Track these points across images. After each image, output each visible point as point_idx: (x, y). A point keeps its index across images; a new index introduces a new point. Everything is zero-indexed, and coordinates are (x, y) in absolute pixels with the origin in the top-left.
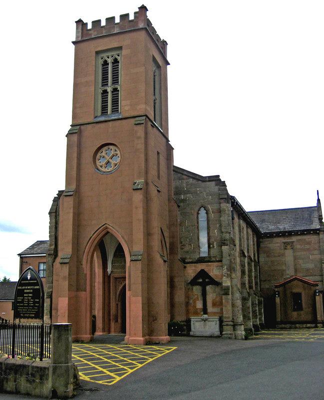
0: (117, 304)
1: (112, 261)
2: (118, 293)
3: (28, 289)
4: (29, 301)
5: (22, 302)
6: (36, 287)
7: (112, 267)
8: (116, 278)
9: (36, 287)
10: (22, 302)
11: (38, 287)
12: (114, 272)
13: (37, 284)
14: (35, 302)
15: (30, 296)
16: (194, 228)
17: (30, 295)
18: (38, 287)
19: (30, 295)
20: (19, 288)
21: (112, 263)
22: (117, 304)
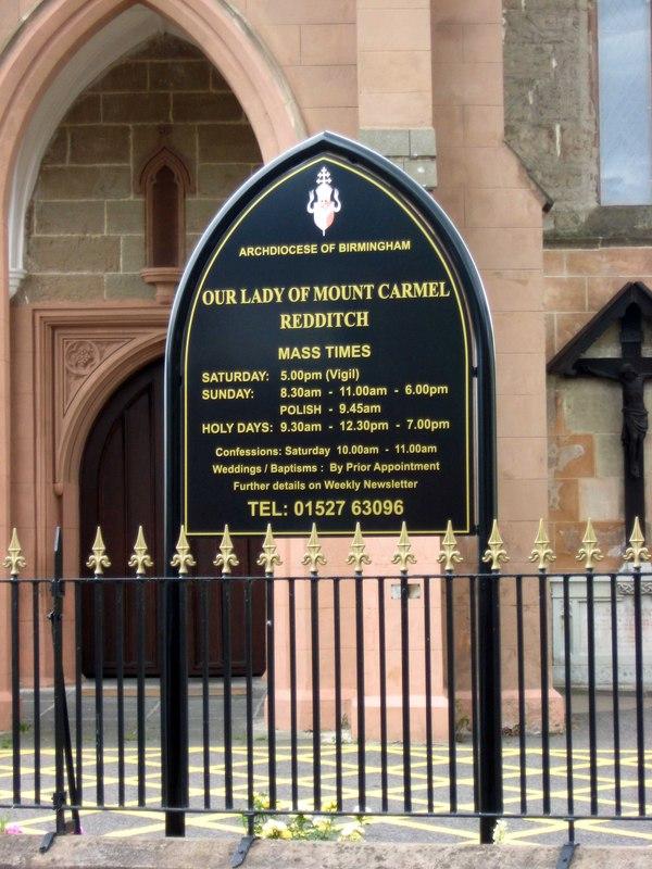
0: (59, 497)
1: (30, 211)
2: (66, 424)
3: (312, 306)
4: (331, 395)
5: (265, 402)
6: (406, 291)
7: (28, 253)
8: (55, 327)
9: (406, 291)
10: (265, 402)
11: (428, 290)
12: (38, 279)
13: (420, 265)
14: (396, 408)
15: (345, 364)
16: (570, 20)
17: (344, 352)
18: (428, 290)
19: (344, 352)
20: (213, 297)
21: (29, 227)
22: (59, 497)
